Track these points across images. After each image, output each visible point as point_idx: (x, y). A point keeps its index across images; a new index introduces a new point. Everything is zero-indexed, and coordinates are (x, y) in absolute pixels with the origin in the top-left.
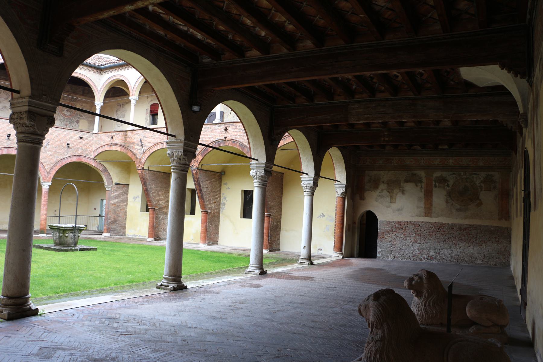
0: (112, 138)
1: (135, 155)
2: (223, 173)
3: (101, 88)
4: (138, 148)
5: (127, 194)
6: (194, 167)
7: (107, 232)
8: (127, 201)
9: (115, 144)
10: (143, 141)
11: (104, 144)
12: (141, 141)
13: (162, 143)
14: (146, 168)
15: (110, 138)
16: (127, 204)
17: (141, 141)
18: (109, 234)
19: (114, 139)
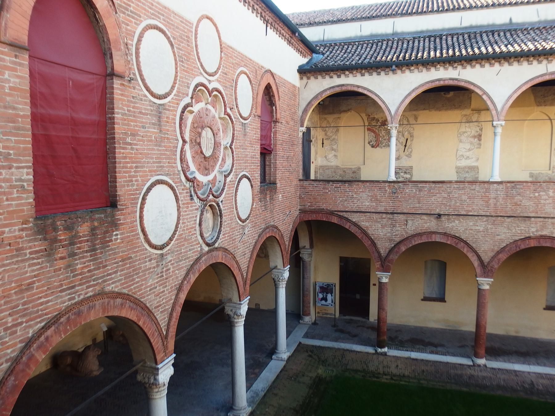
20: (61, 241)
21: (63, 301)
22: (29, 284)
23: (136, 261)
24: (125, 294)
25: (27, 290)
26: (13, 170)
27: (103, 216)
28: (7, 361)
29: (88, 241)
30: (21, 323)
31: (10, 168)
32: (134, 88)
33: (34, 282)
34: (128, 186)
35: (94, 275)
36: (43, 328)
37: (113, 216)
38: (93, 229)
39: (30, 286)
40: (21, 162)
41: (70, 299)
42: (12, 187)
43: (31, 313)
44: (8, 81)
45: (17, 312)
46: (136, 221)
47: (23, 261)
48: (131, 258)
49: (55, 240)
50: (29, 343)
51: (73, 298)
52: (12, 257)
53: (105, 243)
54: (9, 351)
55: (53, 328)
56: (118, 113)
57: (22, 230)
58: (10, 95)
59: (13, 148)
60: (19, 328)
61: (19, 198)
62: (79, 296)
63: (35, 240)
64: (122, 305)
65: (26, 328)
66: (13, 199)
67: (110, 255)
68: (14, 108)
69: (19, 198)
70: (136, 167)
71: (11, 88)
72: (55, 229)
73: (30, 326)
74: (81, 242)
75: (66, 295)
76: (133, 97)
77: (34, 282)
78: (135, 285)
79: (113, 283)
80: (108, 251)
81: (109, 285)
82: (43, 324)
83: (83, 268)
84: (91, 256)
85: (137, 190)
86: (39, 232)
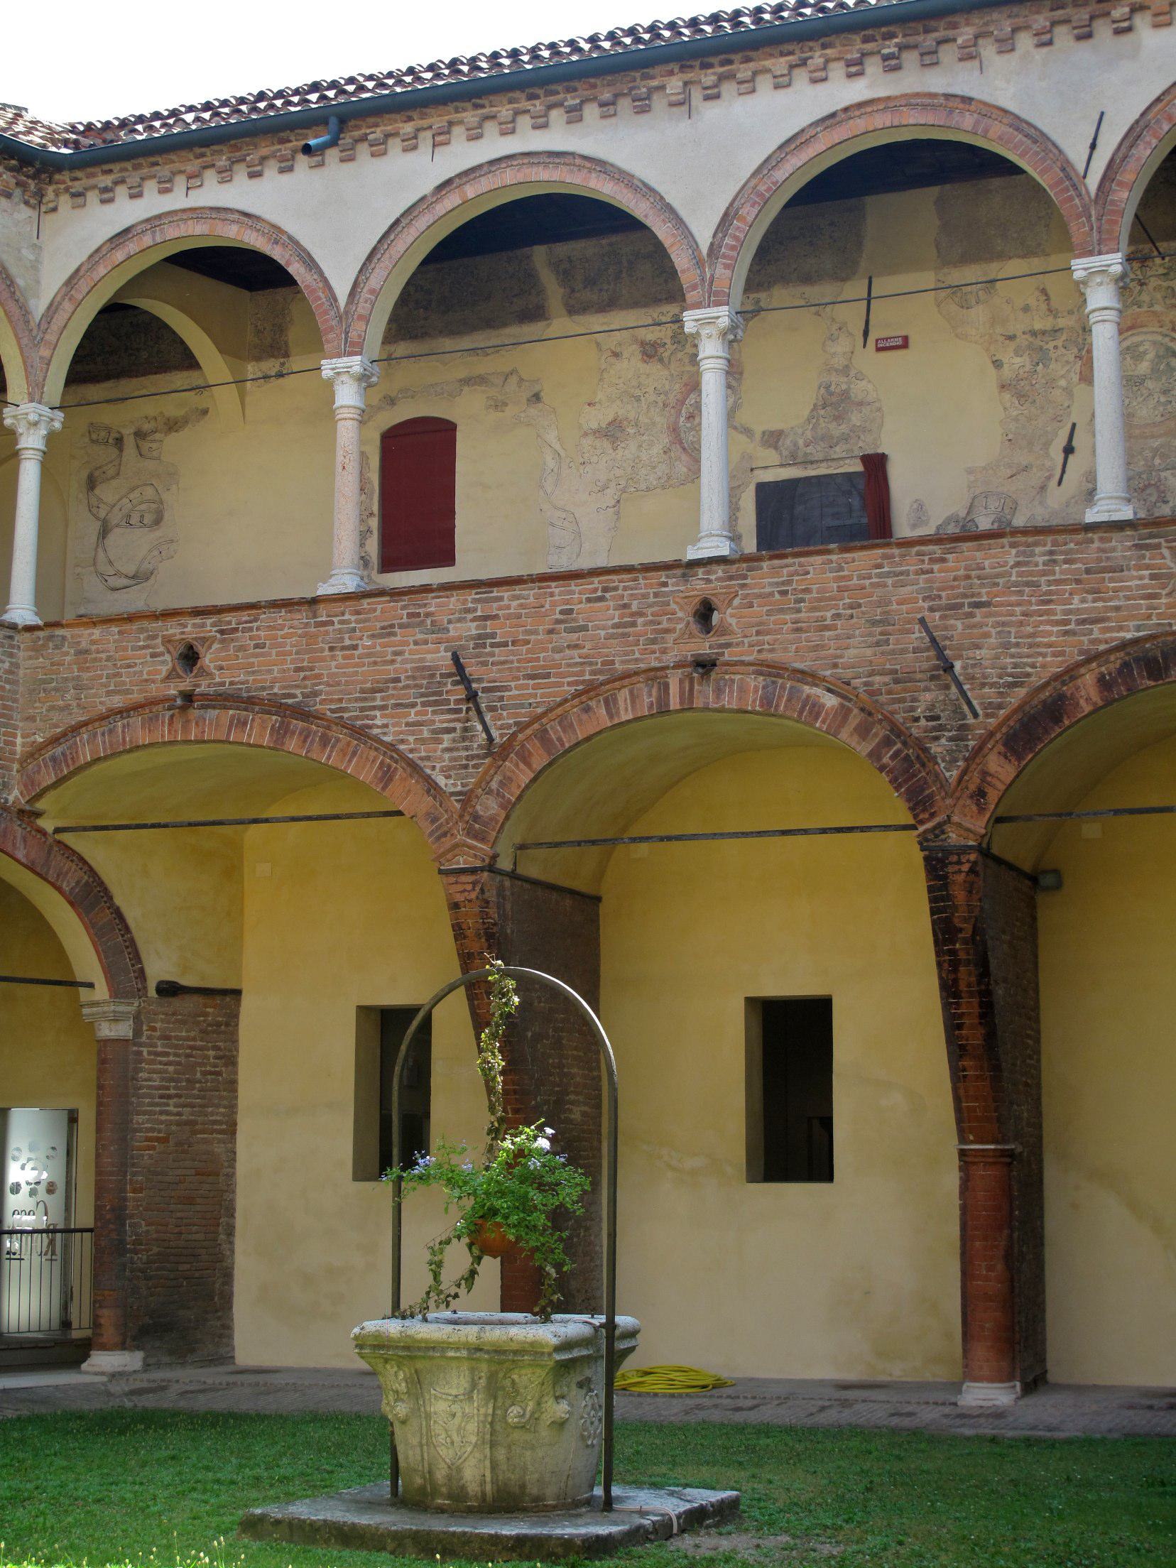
0: (190, 657)
1: (414, 767)
2: (1048, 880)
3: (53, 308)
4: (441, 721)
5: (230, 1061)
6: (953, 837)
7: (122, 1346)
8: (233, 1107)
9: (223, 700)
10: (472, 670)
11: (117, 701)
13: (655, 675)
14: (505, 864)
15: (167, 662)
16: (231, 1130)
18: (128, 1360)
19: (208, 659)
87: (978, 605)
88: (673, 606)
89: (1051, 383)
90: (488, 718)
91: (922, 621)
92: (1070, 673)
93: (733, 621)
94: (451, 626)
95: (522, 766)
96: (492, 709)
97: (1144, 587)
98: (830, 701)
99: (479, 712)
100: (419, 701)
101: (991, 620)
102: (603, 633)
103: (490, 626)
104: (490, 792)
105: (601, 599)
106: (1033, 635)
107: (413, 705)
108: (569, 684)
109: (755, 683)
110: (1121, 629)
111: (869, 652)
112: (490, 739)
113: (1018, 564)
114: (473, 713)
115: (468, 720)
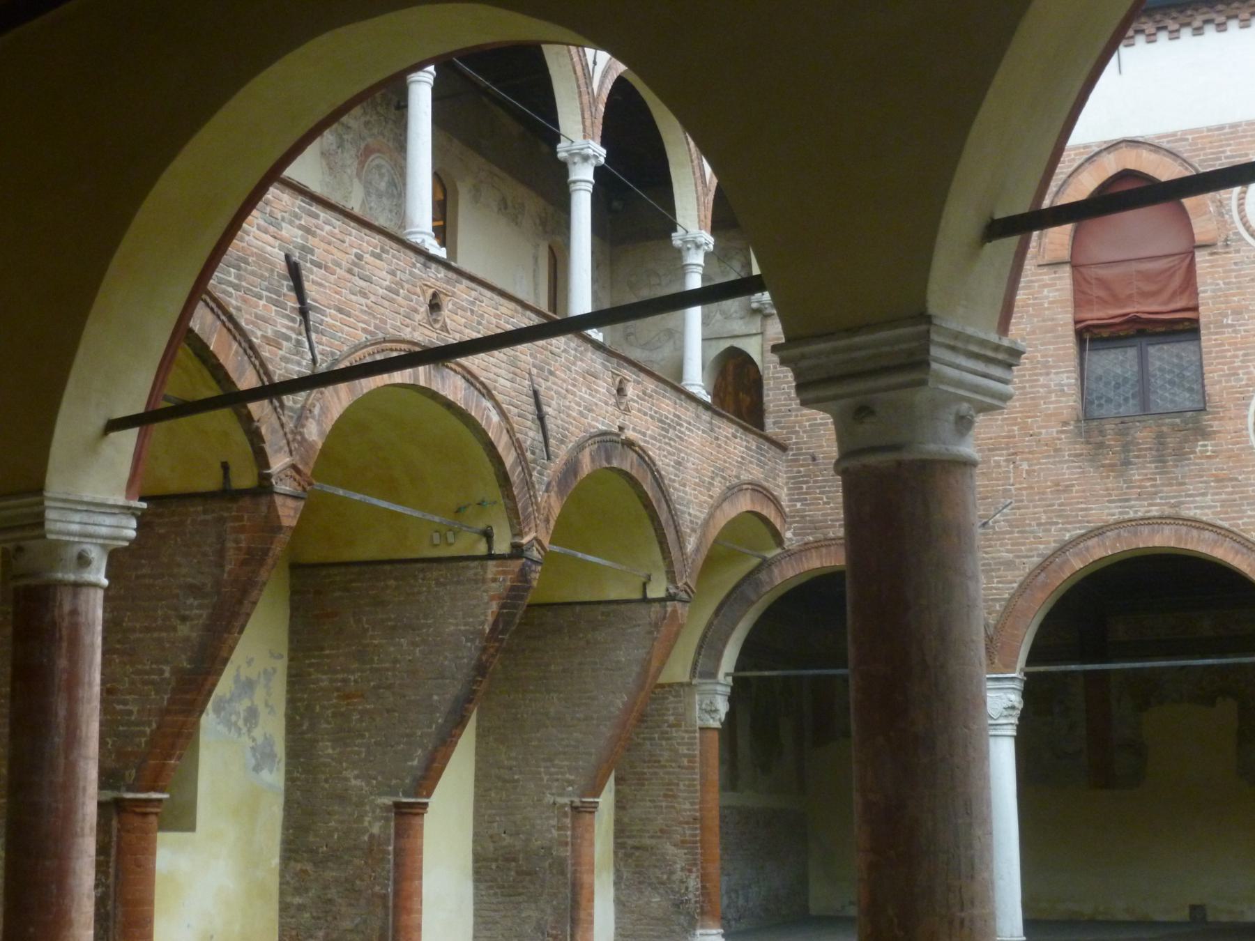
12: (294, 271)
17: (294, 271)
20: (1109, 446)
21: (1112, 513)
22: (1067, 486)
23: (1246, 485)
24: (1221, 528)
25: (1064, 491)
26: (1052, 376)
27: (1178, 420)
28: (1039, 555)
29: (1151, 449)
30: (1057, 523)
31: (1048, 374)
32: (1238, 251)
33: (1073, 485)
34: (1227, 382)
35: (1161, 492)
36: (1083, 535)
37: (1198, 421)
38: (1160, 438)
39: (1068, 489)
40: (1060, 367)
41: (1120, 513)
42: (1050, 392)
43: (1068, 516)
44: (1047, 297)
45: (1052, 511)
46: (1247, 429)
47: (1060, 462)
48: (1236, 479)
49: (1101, 445)
50: (1063, 548)
51: (1128, 513)
52: (1048, 457)
53: (1180, 455)
54: (1042, 546)
55: (1096, 539)
56: (1205, 292)
57: (1062, 432)
58: (1048, 309)
59: (1052, 356)
60: (1053, 528)
61: (1056, 402)
62: (1136, 512)
63: (1075, 443)
64: (1216, 542)
65: (1061, 530)
66: (1051, 403)
67: (1191, 471)
68: (1053, 319)
69: (1056, 402)
70: (1245, 355)
71: (1050, 303)
72: (1102, 433)
73: (1067, 530)
74: (1140, 450)
75: (1117, 507)
76: (1236, 264)
77: (1073, 485)
78: (1246, 520)
79: (1196, 508)
80: (1188, 465)
81: (1189, 509)
82: (1083, 531)
83: (1142, 480)
84: (1156, 468)
85: (1247, 385)
86: (1080, 435)
87: (551, 373)
88: (418, 290)
89: (343, 166)
90: (314, 336)
91: (530, 374)
92: (580, 447)
93: (448, 320)
94: (284, 225)
95: (336, 399)
96: (317, 332)
97: (604, 395)
98: (495, 417)
99: (308, 330)
100: (264, 293)
101: (555, 387)
102: (381, 292)
103: (312, 241)
104: (313, 417)
105: (379, 257)
106: (568, 408)
107: (260, 298)
108: (364, 330)
109: (460, 382)
110: (597, 421)
111: (508, 384)
112: (314, 360)
113: (565, 351)
114: (303, 327)
115: (300, 334)
